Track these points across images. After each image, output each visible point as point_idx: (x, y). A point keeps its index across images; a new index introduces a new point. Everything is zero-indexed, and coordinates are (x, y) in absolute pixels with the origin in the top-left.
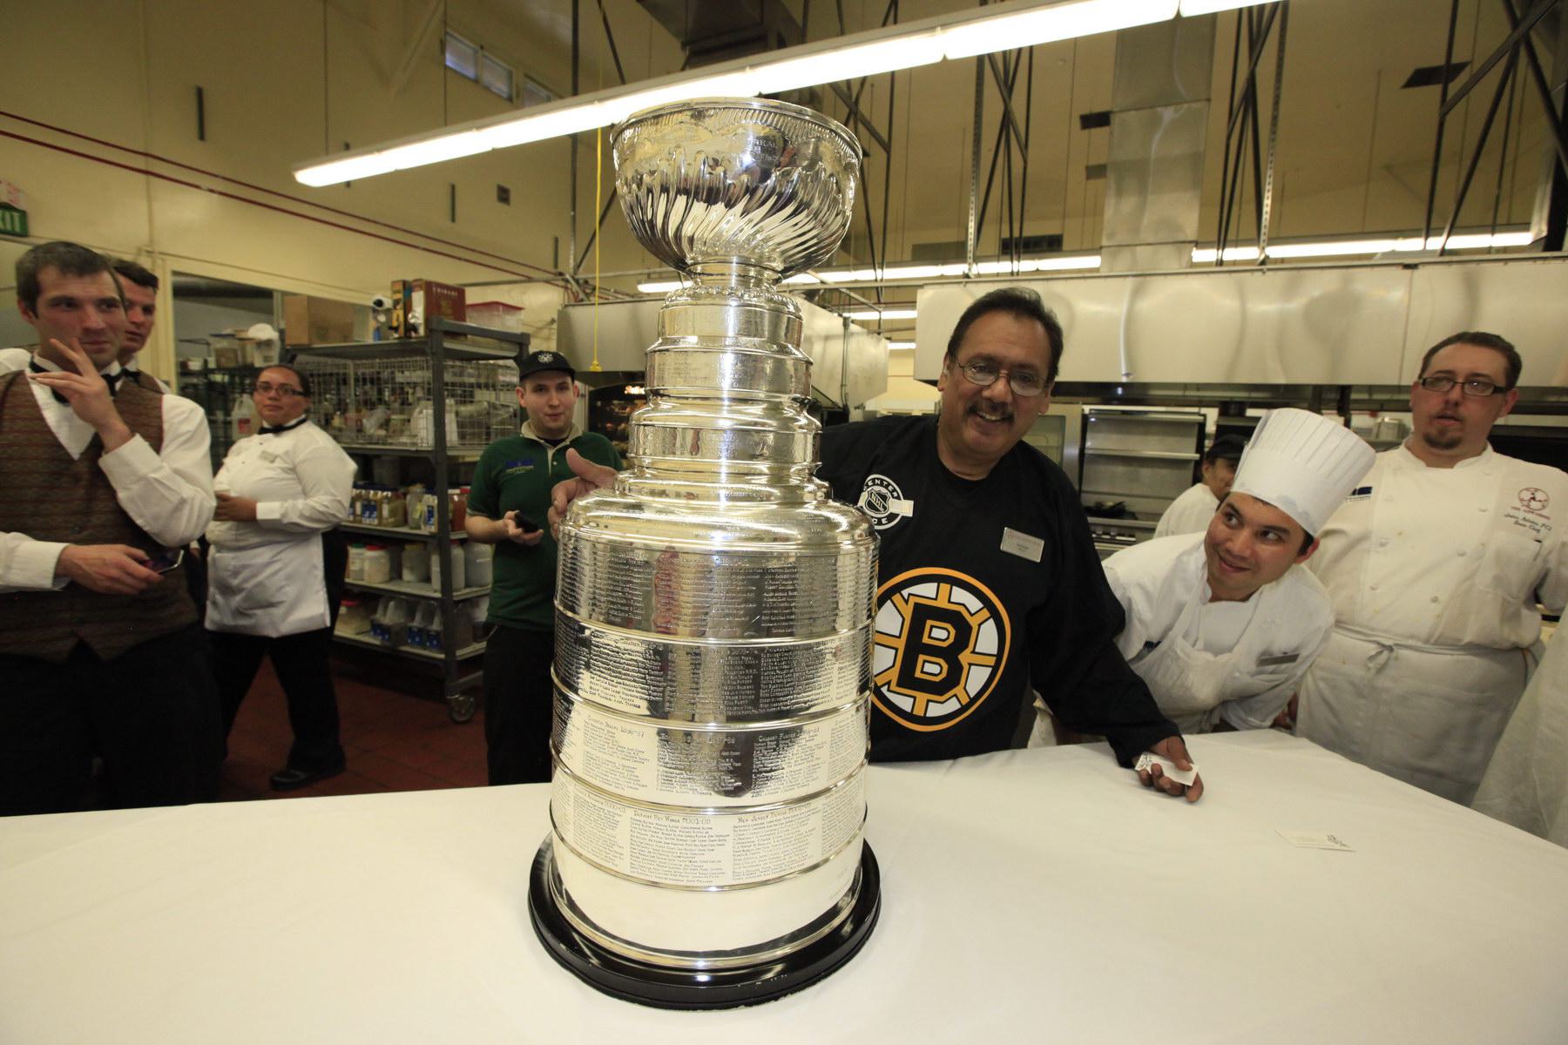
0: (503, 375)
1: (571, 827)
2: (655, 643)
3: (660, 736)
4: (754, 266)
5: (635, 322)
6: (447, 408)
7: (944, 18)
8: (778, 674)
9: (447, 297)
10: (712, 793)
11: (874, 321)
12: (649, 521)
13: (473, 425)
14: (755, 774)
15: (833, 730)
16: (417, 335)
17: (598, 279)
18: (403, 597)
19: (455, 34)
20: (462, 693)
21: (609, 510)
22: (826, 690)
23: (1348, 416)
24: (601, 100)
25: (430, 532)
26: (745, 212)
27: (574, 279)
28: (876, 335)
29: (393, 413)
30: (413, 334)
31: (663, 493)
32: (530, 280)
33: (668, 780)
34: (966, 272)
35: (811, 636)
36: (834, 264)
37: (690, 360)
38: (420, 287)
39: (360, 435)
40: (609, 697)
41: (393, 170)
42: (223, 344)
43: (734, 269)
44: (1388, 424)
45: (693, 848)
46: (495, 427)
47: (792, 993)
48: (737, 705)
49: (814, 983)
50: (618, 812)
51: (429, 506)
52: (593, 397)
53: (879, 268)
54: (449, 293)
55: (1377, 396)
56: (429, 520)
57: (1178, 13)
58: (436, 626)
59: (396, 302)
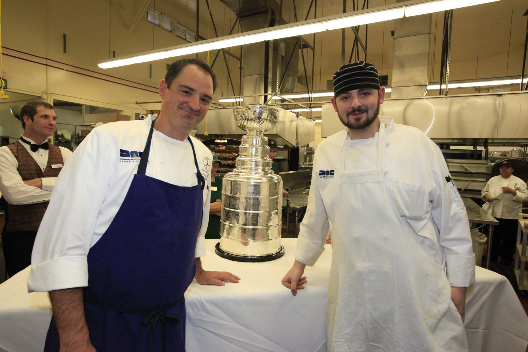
5: (218, 116)
11: (309, 112)
12: (241, 177)
19: (151, 9)
23: (487, 149)
24: (209, 42)
31: (242, 173)
36: (294, 92)
41: (133, 63)
43: (255, 132)
44: (514, 150)
55: (495, 141)
57: (405, 15)
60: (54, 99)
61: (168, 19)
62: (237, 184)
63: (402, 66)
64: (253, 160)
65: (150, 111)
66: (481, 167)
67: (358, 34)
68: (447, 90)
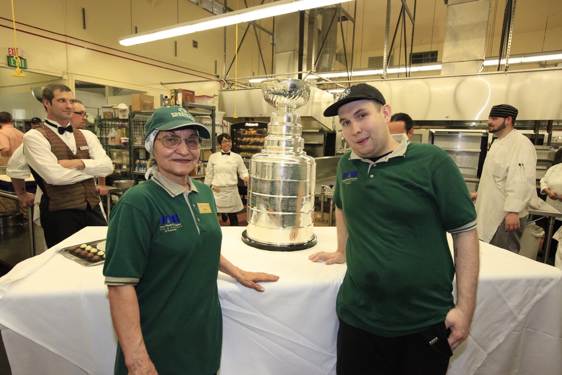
0: (205, 121)
4: (290, 108)
5: (249, 97)
9: (189, 95)
26: (288, 98)
27: (224, 79)
31: (271, 153)
36: (332, 70)
37: (277, 127)
41: (157, 39)
42: (107, 110)
43: (286, 108)
49: (300, 250)
52: (232, 127)
53: (349, 71)
55: (560, 124)
59: (172, 97)
60: (76, 79)
62: (265, 166)
63: (455, 37)
64: (283, 140)
66: (542, 153)
67: (406, 2)
68: (507, 65)
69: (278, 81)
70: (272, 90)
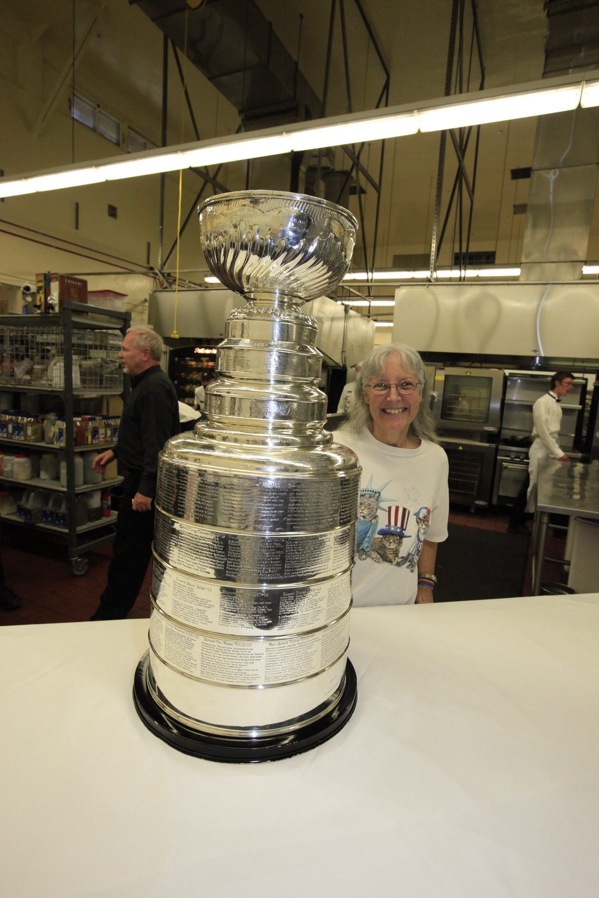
0: (113, 340)
1: (163, 648)
2: (220, 533)
3: (222, 591)
4: (287, 295)
6: (74, 362)
7: (420, 104)
8: (296, 554)
9: (75, 286)
10: (254, 627)
12: (218, 457)
13: (91, 374)
14: (281, 615)
15: (329, 589)
16: (54, 312)
17: (178, 274)
18: (41, 490)
20: (80, 556)
21: (192, 449)
22: (325, 564)
24: (183, 150)
25: (61, 447)
26: (284, 262)
27: (161, 273)
28: (366, 318)
29: (34, 365)
30: (51, 311)
32: (131, 272)
33: (226, 619)
34: (429, 277)
35: (317, 531)
37: (245, 355)
38: (57, 280)
39: (12, 378)
40: (190, 566)
41: (35, 191)
45: (241, 661)
46: (106, 375)
47: (300, 753)
48: (270, 573)
49: (314, 747)
50: (194, 638)
51: (59, 429)
52: (172, 354)
53: (370, 272)
54: (76, 283)
56: (60, 438)
58: (63, 509)
59: (39, 289)
61: (112, 120)
65: (43, 276)
69: (251, 202)
70: (232, 231)
